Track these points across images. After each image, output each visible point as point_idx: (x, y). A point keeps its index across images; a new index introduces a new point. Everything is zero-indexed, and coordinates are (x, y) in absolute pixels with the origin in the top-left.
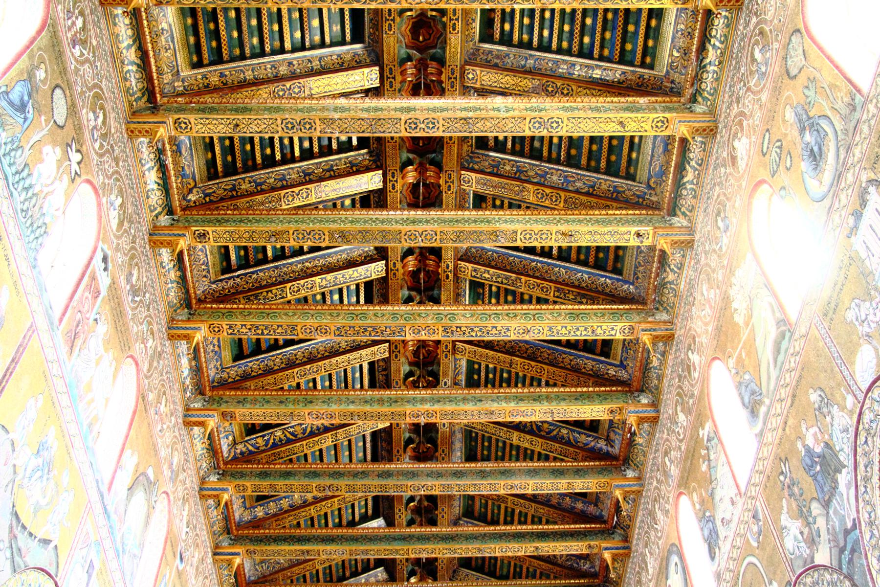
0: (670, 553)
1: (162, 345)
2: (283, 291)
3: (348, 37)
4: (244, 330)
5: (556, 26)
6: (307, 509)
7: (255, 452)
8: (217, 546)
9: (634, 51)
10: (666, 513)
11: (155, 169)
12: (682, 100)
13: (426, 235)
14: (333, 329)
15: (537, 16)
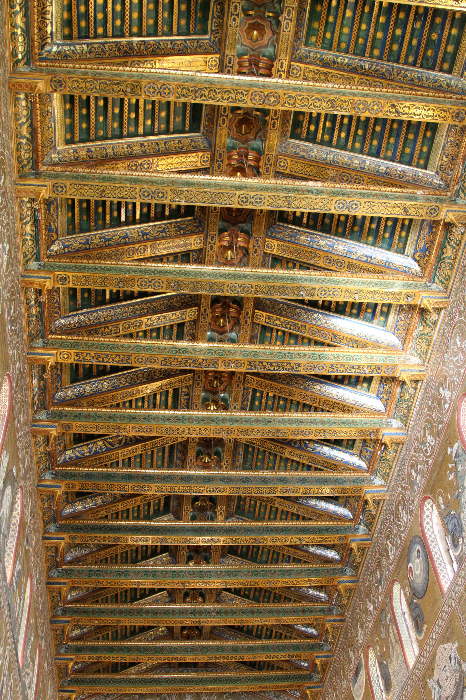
0: (412, 543)
1: (24, 367)
2: (117, 327)
3: (187, 128)
4: (88, 358)
5: (353, 130)
6: (116, 504)
7: (80, 458)
8: (45, 532)
9: (412, 155)
10: (410, 512)
11: (30, 223)
12: (449, 194)
13: (245, 287)
14: (160, 359)
15: (338, 121)
